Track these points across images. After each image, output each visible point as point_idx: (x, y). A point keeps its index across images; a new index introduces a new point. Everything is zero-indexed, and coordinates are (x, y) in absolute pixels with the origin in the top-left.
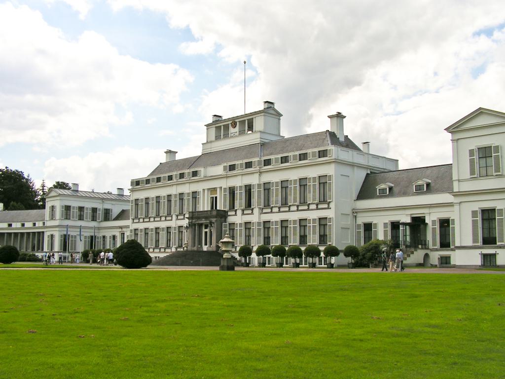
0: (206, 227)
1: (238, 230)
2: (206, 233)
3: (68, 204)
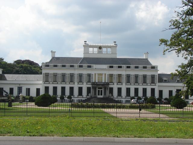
0: (99, 88)
2: (99, 91)
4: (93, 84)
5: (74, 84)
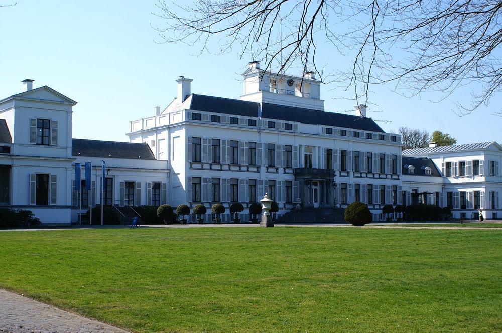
1: (282, 187)
3: (44, 115)
4: (298, 173)
5: (258, 171)
